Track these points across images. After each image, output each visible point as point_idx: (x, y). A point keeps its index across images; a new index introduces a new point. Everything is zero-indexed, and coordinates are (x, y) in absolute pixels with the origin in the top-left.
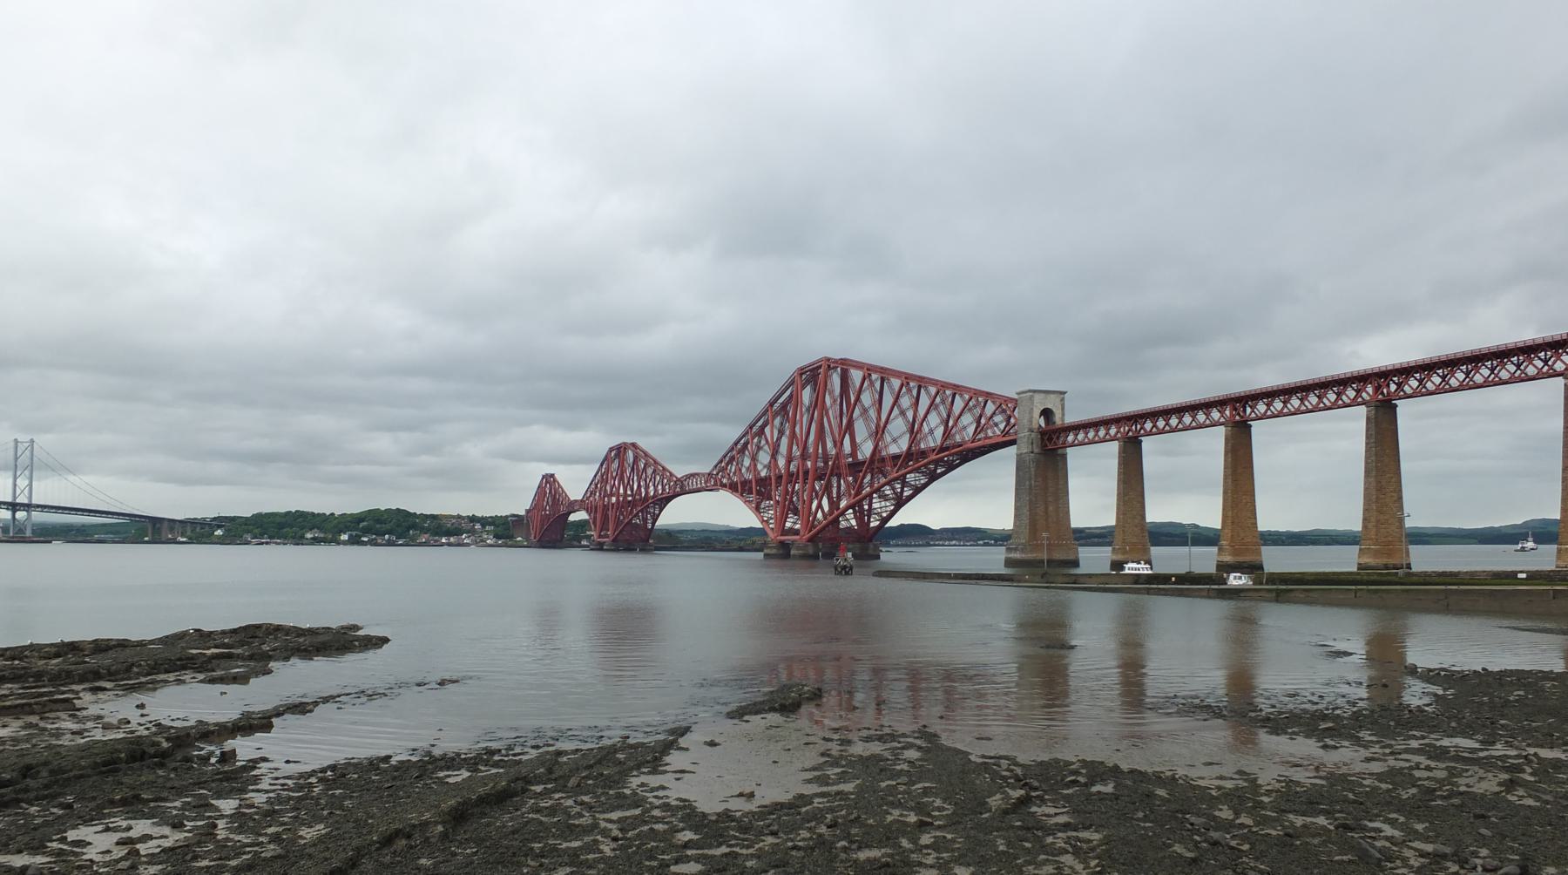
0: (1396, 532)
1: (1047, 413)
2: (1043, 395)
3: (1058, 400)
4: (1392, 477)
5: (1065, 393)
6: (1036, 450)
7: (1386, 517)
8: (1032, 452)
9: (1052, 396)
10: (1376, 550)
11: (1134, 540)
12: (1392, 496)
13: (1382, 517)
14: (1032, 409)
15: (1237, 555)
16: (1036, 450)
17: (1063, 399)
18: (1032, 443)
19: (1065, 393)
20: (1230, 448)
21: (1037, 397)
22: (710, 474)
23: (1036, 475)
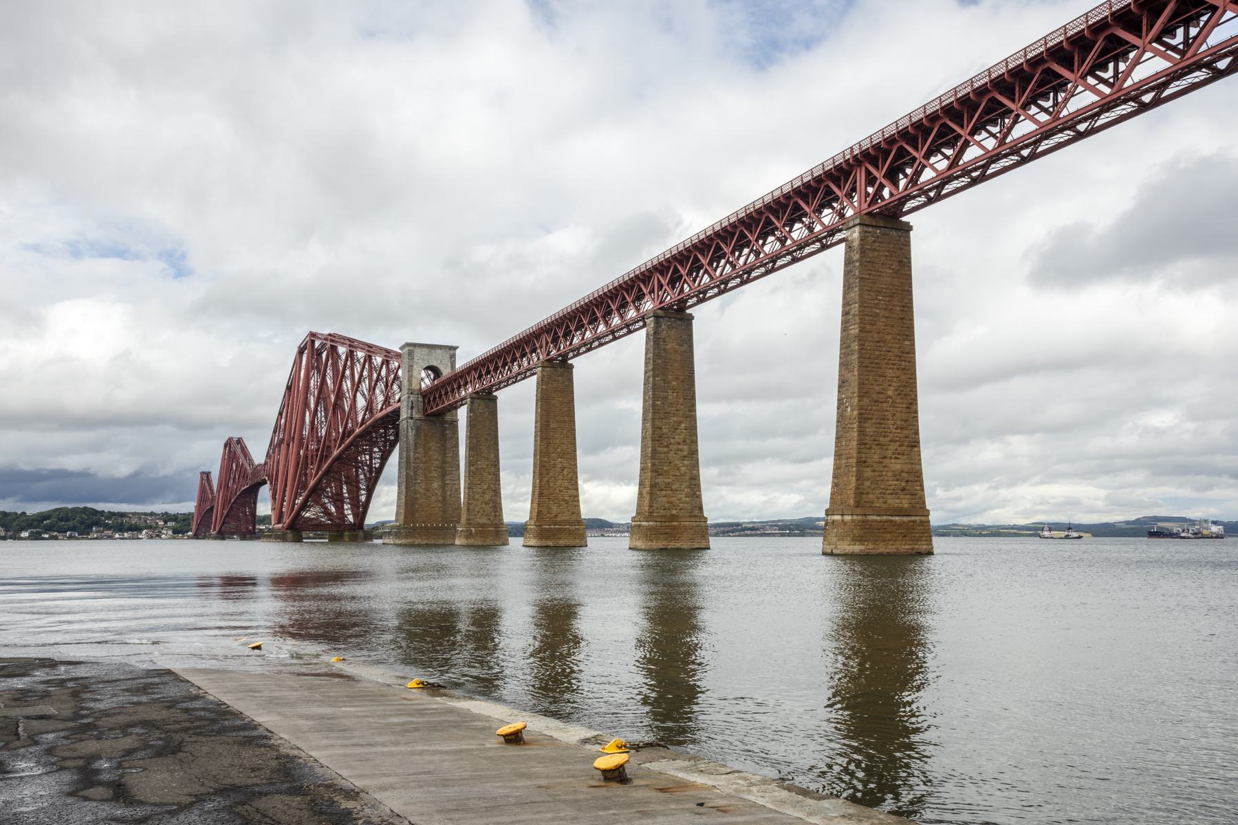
0: (686, 502)
1: (435, 370)
2: (426, 350)
3: (448, 356)
4: (681, 422)
5: (455, 348)
6: (416, 416)
7: (668, 481)
8: (412, 418)
9: (439, 351)
10: (650, 529)
11: (484, 521)
12: (681, 450)
13: (660, 480)
14: (412, 366)
15: (547, 538)
16: (416, 416)
17: (453, 357)
18: (412, 408)
19: (455, 348)
20: (539, 395)
21: (418, 353)
22: (266, 463)
23: (415, 445)
